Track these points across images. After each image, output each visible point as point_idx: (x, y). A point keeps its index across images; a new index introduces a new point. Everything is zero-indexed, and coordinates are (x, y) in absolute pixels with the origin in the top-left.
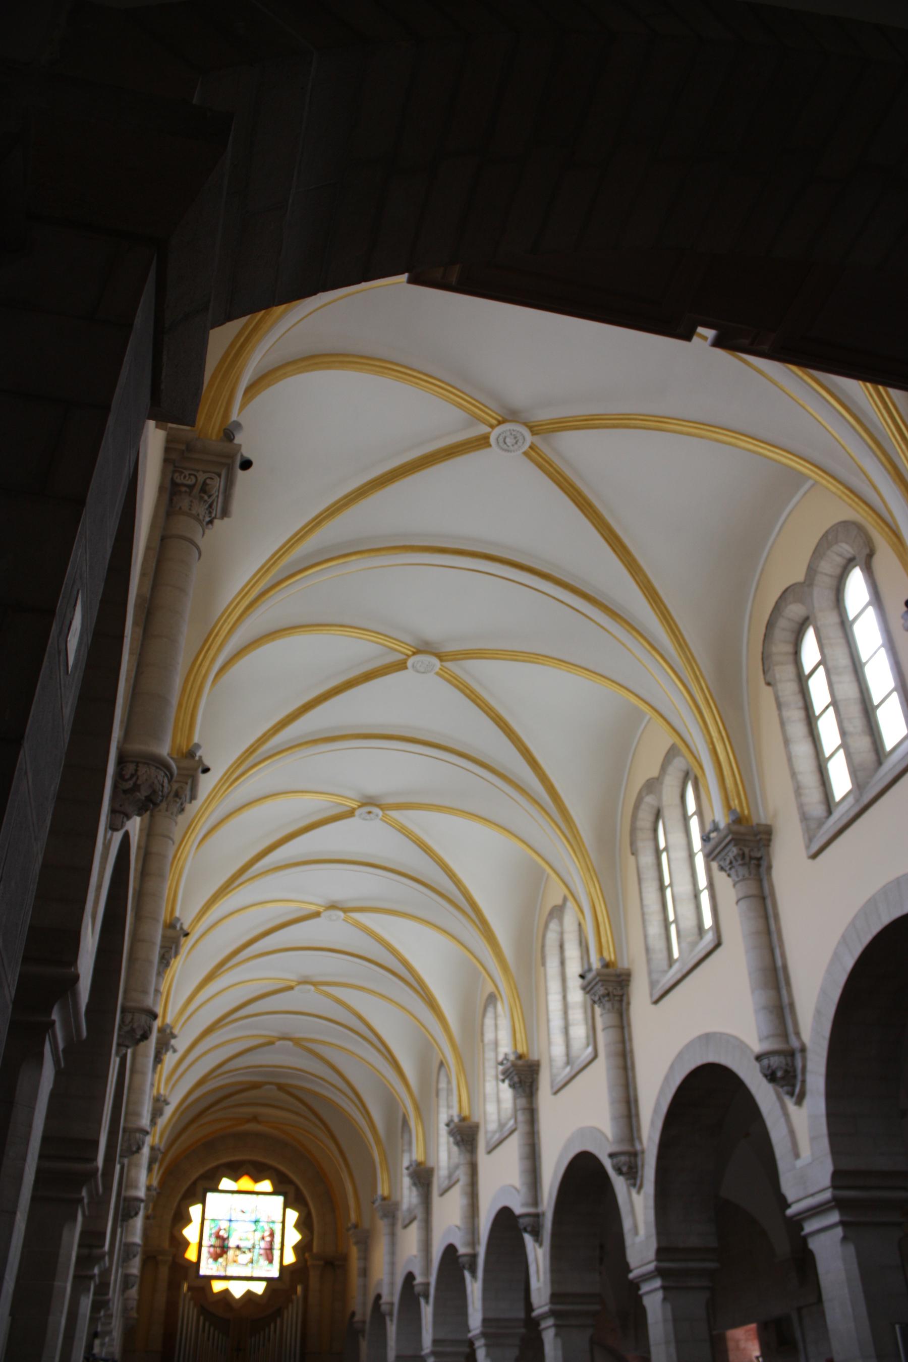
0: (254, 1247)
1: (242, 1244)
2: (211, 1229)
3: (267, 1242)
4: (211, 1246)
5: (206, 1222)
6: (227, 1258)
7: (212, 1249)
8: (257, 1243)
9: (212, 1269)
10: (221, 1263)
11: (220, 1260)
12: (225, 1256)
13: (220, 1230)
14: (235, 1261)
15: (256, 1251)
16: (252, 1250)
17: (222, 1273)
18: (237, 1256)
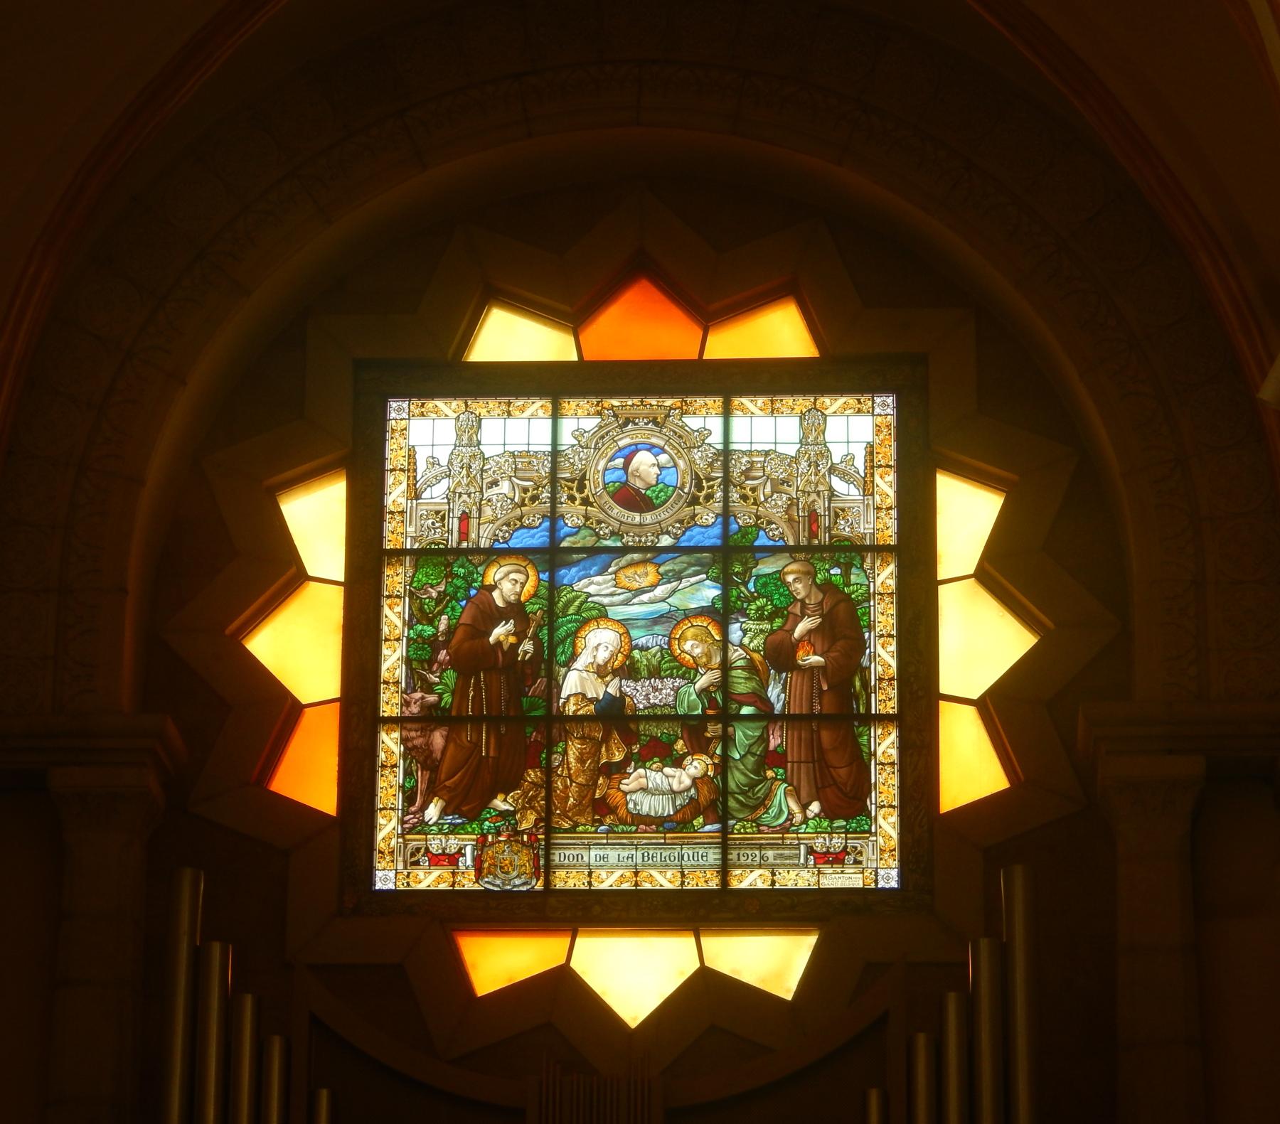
0: (727, 718)
1: (641, 695)
2: (419, 615)
3: (812, 669)
4: (430, 718)
5: (395, 579)
6: (548, 785)
7: (438, 739)
8: (742, 685)
9: (452, 859)
10: (503, 815)
11: (500, 803)
12: (532, 775)
13: (497, 616)
14: (602, 808)
15: (743, 735)
16: (713, 730)
17: (519, 881)
18: (616, 771)
